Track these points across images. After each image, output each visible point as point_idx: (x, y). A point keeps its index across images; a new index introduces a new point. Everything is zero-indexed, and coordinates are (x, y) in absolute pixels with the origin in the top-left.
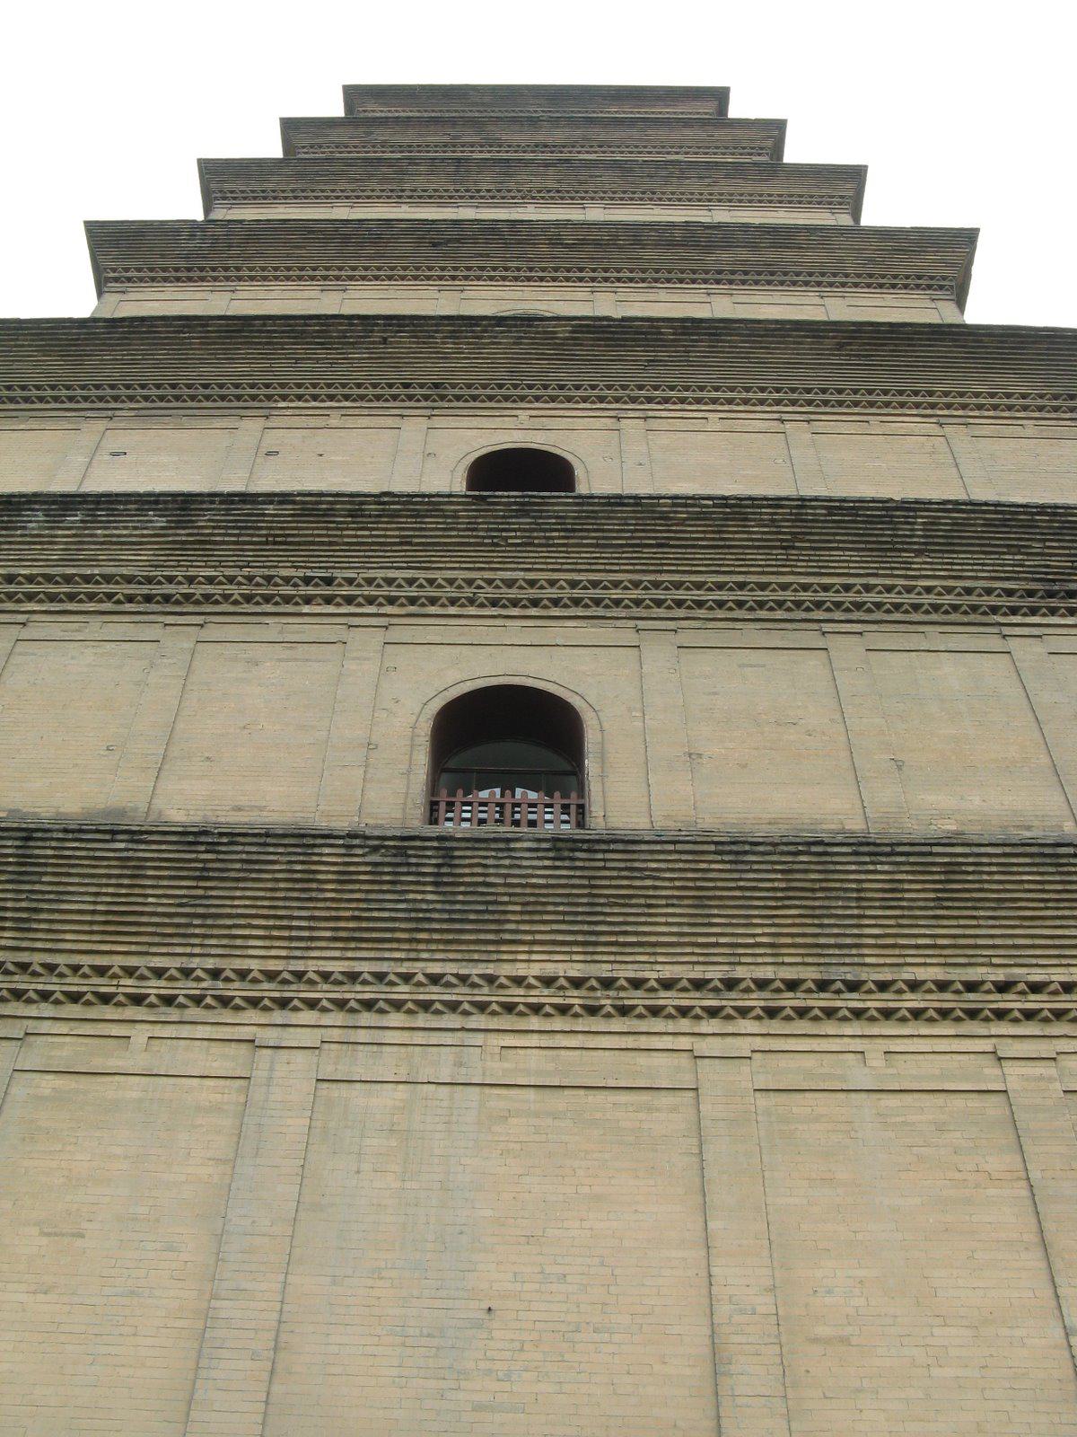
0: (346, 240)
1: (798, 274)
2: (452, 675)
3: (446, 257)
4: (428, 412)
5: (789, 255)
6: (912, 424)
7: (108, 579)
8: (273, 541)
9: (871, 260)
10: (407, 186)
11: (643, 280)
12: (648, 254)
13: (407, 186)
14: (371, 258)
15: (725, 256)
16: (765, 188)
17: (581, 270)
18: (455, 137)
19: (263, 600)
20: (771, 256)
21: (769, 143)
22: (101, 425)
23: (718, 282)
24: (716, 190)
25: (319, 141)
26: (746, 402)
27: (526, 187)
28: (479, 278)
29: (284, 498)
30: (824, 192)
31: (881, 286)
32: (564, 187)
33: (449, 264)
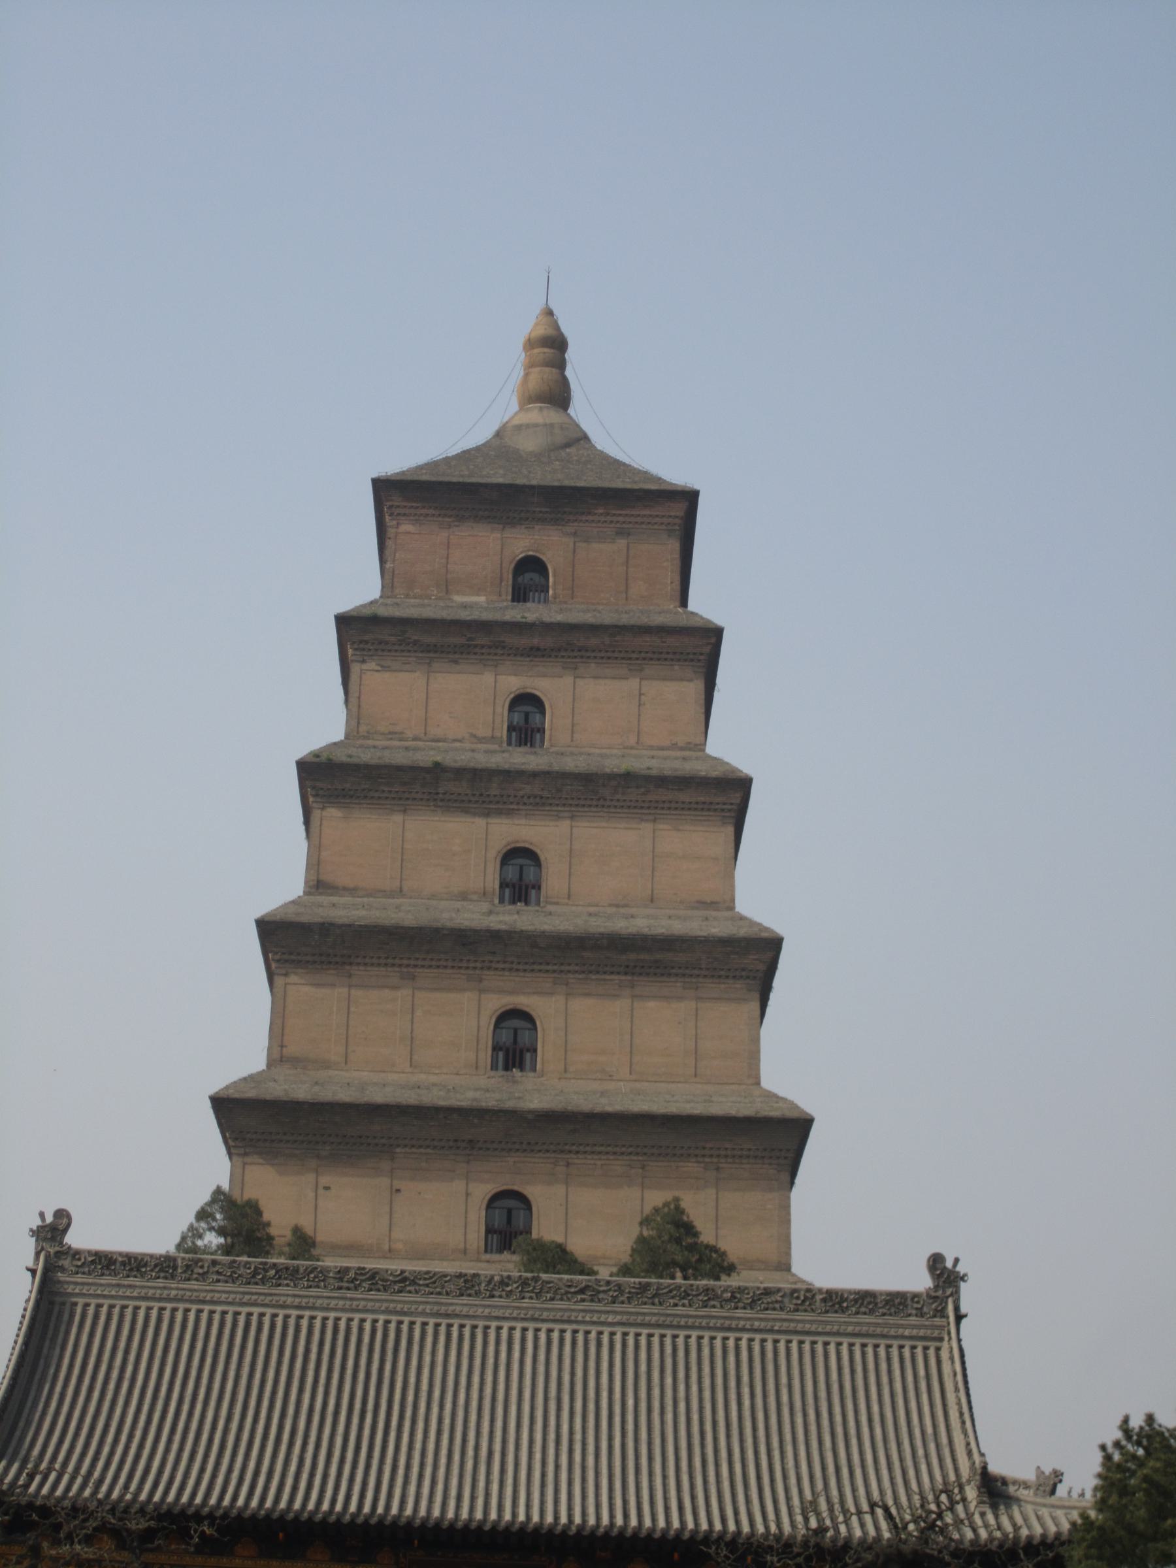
1: (673, 968)
10: (441, 790)
12: (587, 954)
13: (441, 790)
15: (633, 956)
17: (548, 964)
18: (470, 639)
20: (658, 956)
21: (707, 649)
23: (626, 974)
25: (366, 638)
26: (615, 1153)
27: (521, 793)
28: (489, 968)
30: (720, 800)
31: (720, 977)
32: (545, 794)
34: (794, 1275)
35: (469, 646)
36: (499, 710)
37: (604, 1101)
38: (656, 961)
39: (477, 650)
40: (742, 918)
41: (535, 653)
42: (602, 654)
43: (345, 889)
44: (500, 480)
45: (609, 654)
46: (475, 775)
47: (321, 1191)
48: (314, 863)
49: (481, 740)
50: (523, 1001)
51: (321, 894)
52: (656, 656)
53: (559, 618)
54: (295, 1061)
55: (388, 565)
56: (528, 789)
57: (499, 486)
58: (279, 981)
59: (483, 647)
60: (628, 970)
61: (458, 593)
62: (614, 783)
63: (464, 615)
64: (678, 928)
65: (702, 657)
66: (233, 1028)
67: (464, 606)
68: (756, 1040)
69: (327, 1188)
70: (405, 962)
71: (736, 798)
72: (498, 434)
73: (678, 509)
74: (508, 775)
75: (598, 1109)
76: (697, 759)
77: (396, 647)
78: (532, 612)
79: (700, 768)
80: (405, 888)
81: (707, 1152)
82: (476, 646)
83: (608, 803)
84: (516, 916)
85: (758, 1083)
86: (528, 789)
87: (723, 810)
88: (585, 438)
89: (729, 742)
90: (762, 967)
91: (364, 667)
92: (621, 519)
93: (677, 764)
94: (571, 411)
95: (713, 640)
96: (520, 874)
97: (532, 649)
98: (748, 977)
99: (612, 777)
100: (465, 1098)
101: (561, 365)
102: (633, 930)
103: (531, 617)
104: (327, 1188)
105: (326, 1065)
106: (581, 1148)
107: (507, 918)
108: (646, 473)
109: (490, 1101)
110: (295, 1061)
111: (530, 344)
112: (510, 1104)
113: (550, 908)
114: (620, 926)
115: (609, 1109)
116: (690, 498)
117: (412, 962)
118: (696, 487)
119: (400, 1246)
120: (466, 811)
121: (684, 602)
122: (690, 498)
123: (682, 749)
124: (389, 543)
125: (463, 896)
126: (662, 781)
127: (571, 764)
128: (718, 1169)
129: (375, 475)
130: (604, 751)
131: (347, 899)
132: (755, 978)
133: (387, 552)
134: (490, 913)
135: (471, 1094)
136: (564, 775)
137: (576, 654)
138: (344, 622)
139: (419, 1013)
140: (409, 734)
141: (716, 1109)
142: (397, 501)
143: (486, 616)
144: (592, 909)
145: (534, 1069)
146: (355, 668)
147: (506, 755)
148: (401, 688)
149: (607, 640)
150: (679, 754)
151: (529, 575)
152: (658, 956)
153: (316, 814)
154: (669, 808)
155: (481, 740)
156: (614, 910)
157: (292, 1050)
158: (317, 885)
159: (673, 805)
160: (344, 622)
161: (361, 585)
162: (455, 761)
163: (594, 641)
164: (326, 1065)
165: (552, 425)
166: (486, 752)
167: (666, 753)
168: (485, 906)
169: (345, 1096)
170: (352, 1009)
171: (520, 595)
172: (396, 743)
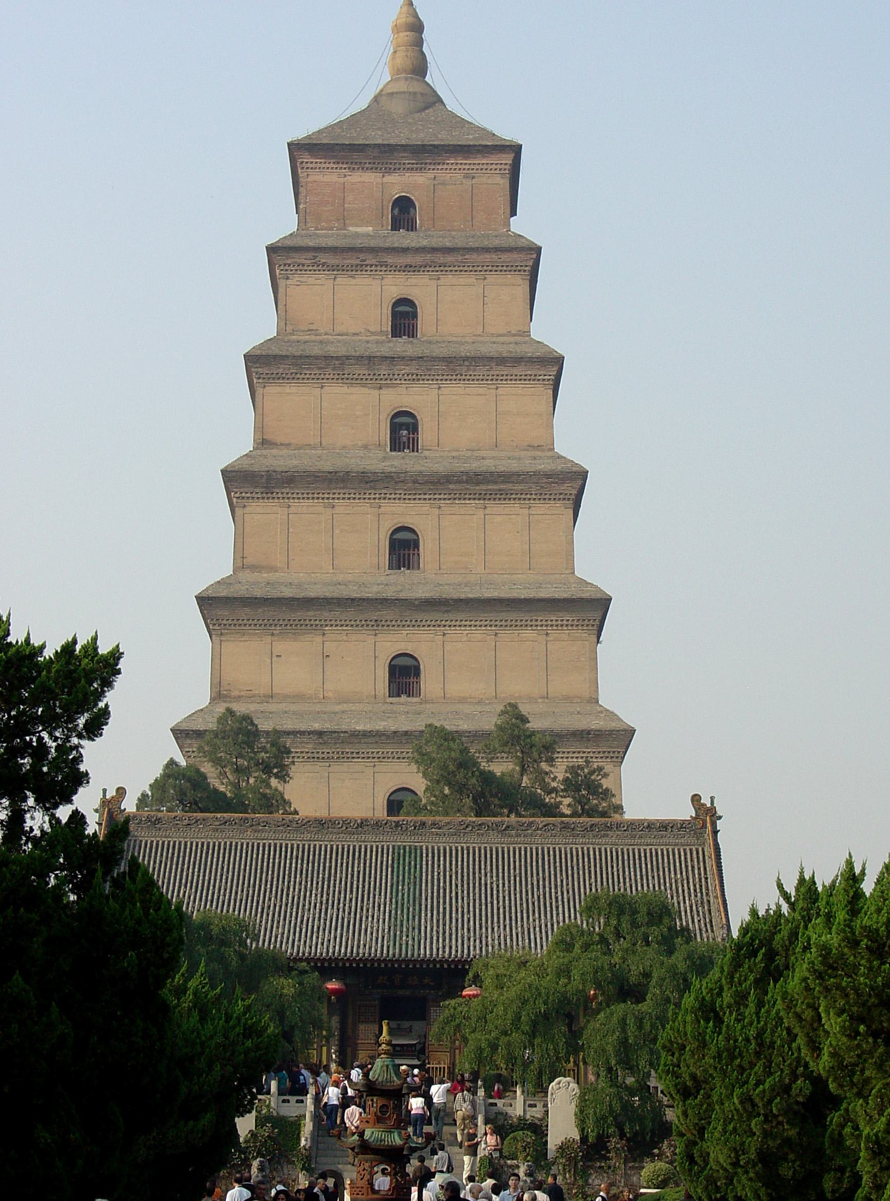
0: (330, 481)
2: (391, 784)
3: (371, 488)
4: (373, 633)
5: (510, 486)
6: (528, 634)
7: (302, 752)
8: (343, 742)
9: (542, 487)
11: (450, 499)
12: (452, 486)
14: (343, 488)
15: (484, 487)
16: (515, 371)
19: (343, 757)
20: (502, 486)
22: (269, 639)
23: (479, 499)
24: (491, 373)
25: (288, 262)
28: (385, 498)
29: (345, 732)
32: (420, 372)
33: (373, 491)
34: (601, 706)
35: (362, 265)
36: (385, 311)
37: (466, 589)
38: (500, 490)
39: (368, 268)
40: (560, 457)
41: (408, 268)
42: (456, 268)
43: (282, 444)
44: (380, 142)
45: (461, 268)
46: (370, 360)
47: (275, 659)
48: (260, 428)
49: (373, 334)
50: (408, 521)
51: (266, 449)
52: (495, 268)
53: (425, 243)
54: (254, 568)
55: (301, 206)
56: (407, 370)
57: (379, 145)
58: (239, 511)
59: (371, 266)
60: (482, 497)
61: (352, 225)
62: (466, 363)
63: (358, 243)
64: (514, 466)
65: (527, 268)
66: (207, 545)
67: (357, 235)
68: (571, 543)
69: (280, 656)
70: (326, 496)
71: (553, 371)
72: (376, 99)
73: (508, 159)
74: (391, 360)
75: (463, 596)
76: (525, 343)
77: (311, 268)
78: (403, 238)
79: (529, 351)
80: (324, 443)
81: (539, 623)
82: (366, 266)
83: (464, 377)
84: (402, 461)
85: (573, 573)
86: (407, 370)
87: (544, 380)
88: (440, 101)
89: (546, 330)
90: (574, 492)
91: (289, 282)
92: (467, 167)
93: (511, 347)
94: (428, 79)
95: (534, 256)
96: (403, 430)
97: (406, 266)
98: (564, 499)
99: (466, 359)
100: (370, 592)
101: (419, 43)
102: (484, 469)
103: (406, 243)
104: (280, 656)
105: (273, 569)
106: (453, 623)
107: (395, 463)
108: (484, 129)
109: (390, 593)
110: (254, 568)
111: (396, 29)
112: (402, 595)
113: (426, 453)
114: (474, 466)
115: (470, 596)
116: (516, 150)
117: (331, 496)
118: (520, 142)
119: (330, 694)
120: (364, 386)
121: (513, 213)
122: (516, 150)
123: (514, 335)
124: (301, 189)
125: (365, 447)
126: (501, 361)
127: (437, 351)
128: (547, 634)
129: (289, 141)
130: (459, 339)
131: (285, 452)
132: (569, 499)
133: (301, 197)
134: (385, 459)
135: (375, 589)
136: (435, 359)
137: (437, 269)
138: (272, 250)
139: (337, 531)
140: (322, 331)
141: (543, 594)
142: (306, 158)
143: (373, 243)
144: (454, 454)
145: (419, 568)
146: (282, 283)
147: (391, 345)
148: (315, 292)
149: (460, 258)
150: (512, 339)
151: (403, 212)
152: (502, 486)
153: (259, 391)
154: (506, 380)
155: (373, 334)
156: (470, 453)
157: (249, 560)
158: (263, 442)
159: (509, 377)
160: (272, 250)
161: (283, 223)
162: (355, 351)
163: (449, 259)
164: (273, 569)
165: (415, 93)
166: (377, 342)
167: (502, 339)
168: (381, 454)
169: (288, 593)
170: (291, 530)
171: (396, 226)
172: (313, 338)
